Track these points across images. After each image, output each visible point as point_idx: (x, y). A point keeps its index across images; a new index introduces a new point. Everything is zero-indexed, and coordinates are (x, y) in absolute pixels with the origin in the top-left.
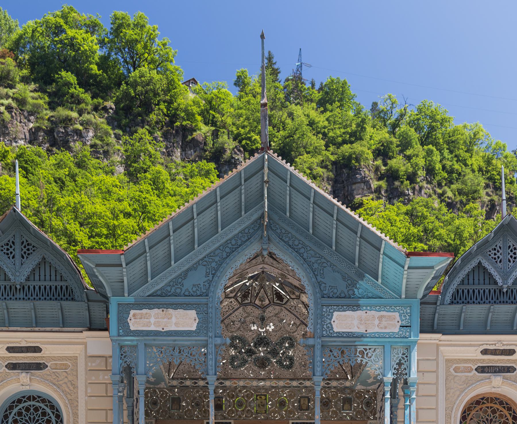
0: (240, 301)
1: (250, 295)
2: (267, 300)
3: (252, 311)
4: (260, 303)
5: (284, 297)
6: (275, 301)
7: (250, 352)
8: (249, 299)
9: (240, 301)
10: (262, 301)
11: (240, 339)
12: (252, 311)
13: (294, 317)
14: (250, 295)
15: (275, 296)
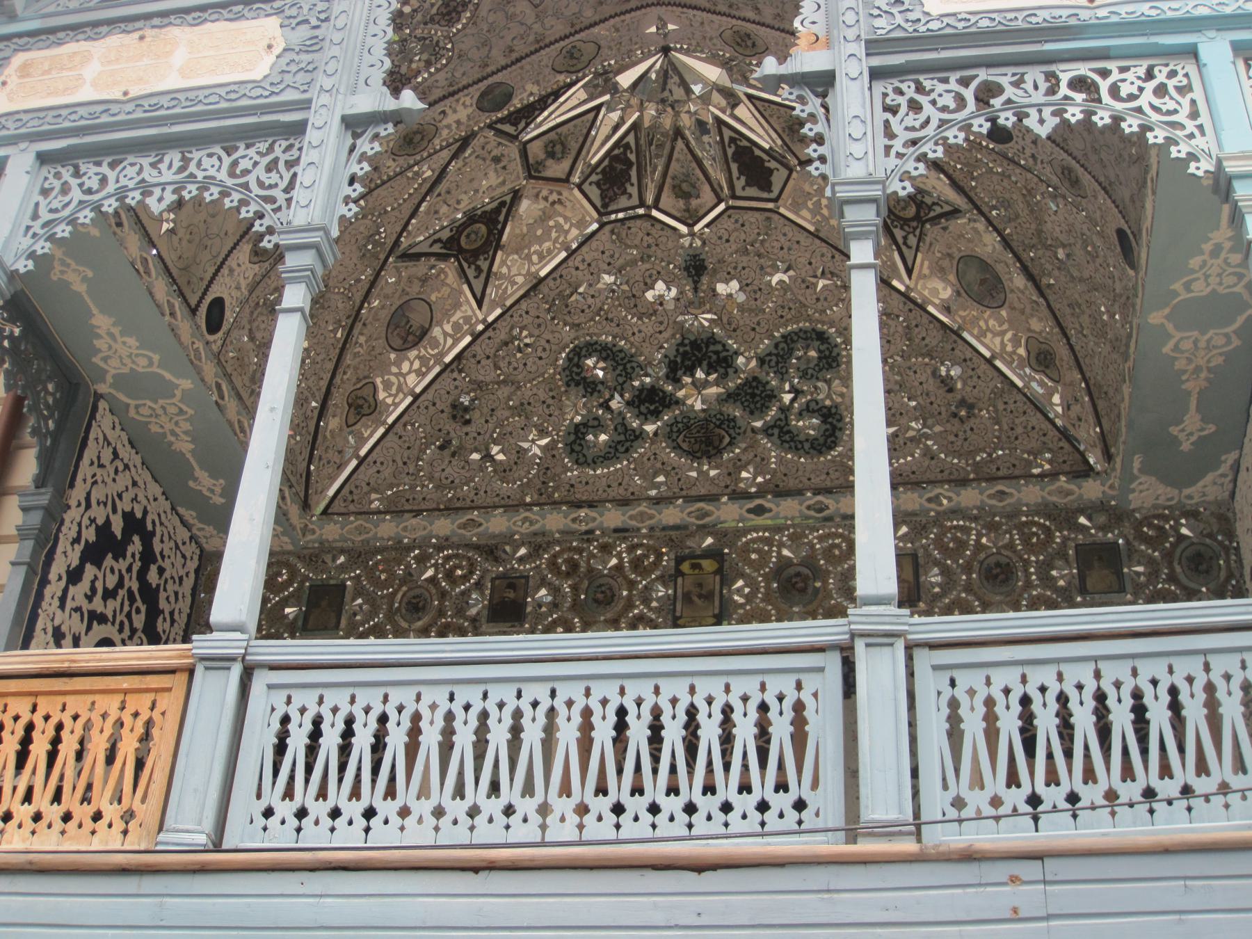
0: (599, 204)
1: (634, 173)
2: (707, 188)
3: (650, 240)
4: (681, 203)
5: (773, 164)
6: (739, 192)
7: (651, 401)
8: (633, 190)
9: (599, 204)
10: (686, 196)
11: (607, 353)
12: (650, 240)
13: (825, 249)
14: (634, 173)
15: (734, 167)
